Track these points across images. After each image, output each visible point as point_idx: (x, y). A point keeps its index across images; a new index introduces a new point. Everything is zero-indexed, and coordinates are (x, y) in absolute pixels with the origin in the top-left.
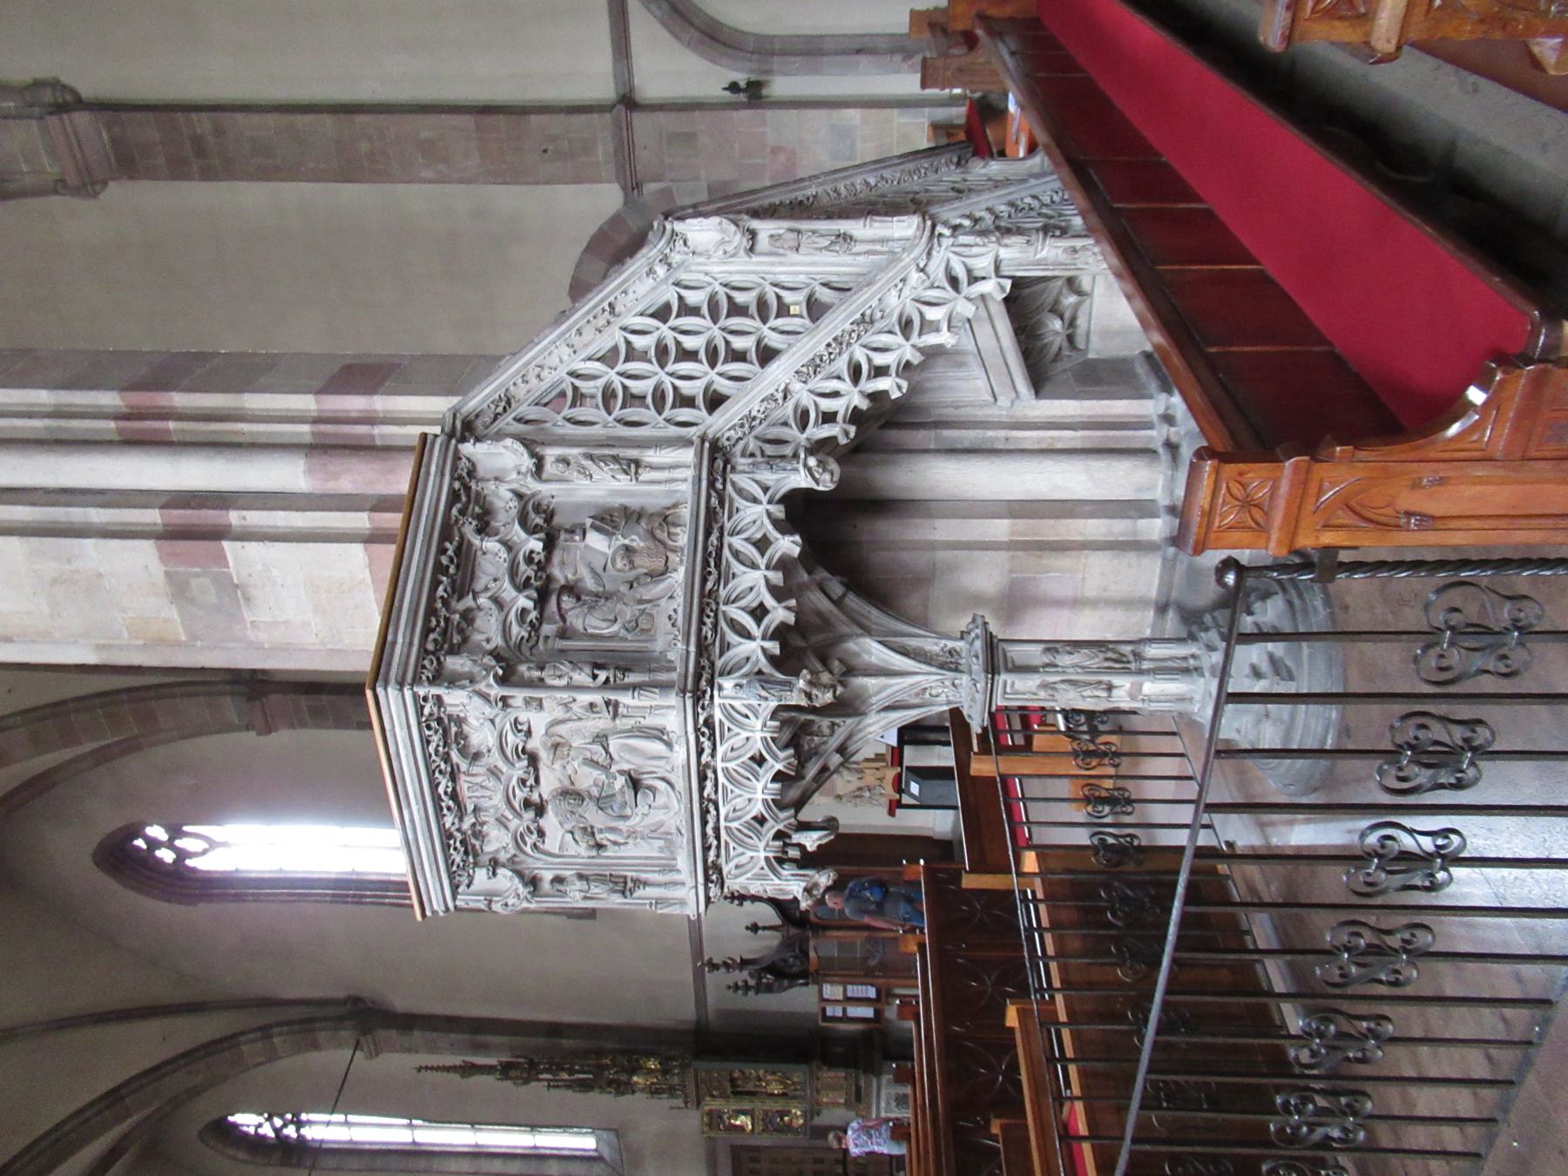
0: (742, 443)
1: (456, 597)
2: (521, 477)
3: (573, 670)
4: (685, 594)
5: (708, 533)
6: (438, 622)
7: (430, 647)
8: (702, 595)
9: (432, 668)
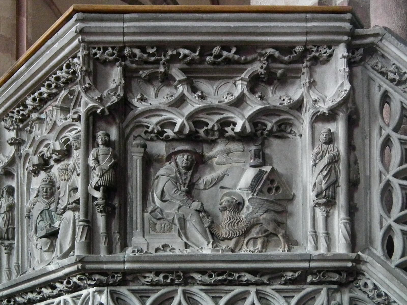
0: (365, 297)
1: (185, 66)
5: (253, 272)
6: (153, 55)
8: (186, 272)
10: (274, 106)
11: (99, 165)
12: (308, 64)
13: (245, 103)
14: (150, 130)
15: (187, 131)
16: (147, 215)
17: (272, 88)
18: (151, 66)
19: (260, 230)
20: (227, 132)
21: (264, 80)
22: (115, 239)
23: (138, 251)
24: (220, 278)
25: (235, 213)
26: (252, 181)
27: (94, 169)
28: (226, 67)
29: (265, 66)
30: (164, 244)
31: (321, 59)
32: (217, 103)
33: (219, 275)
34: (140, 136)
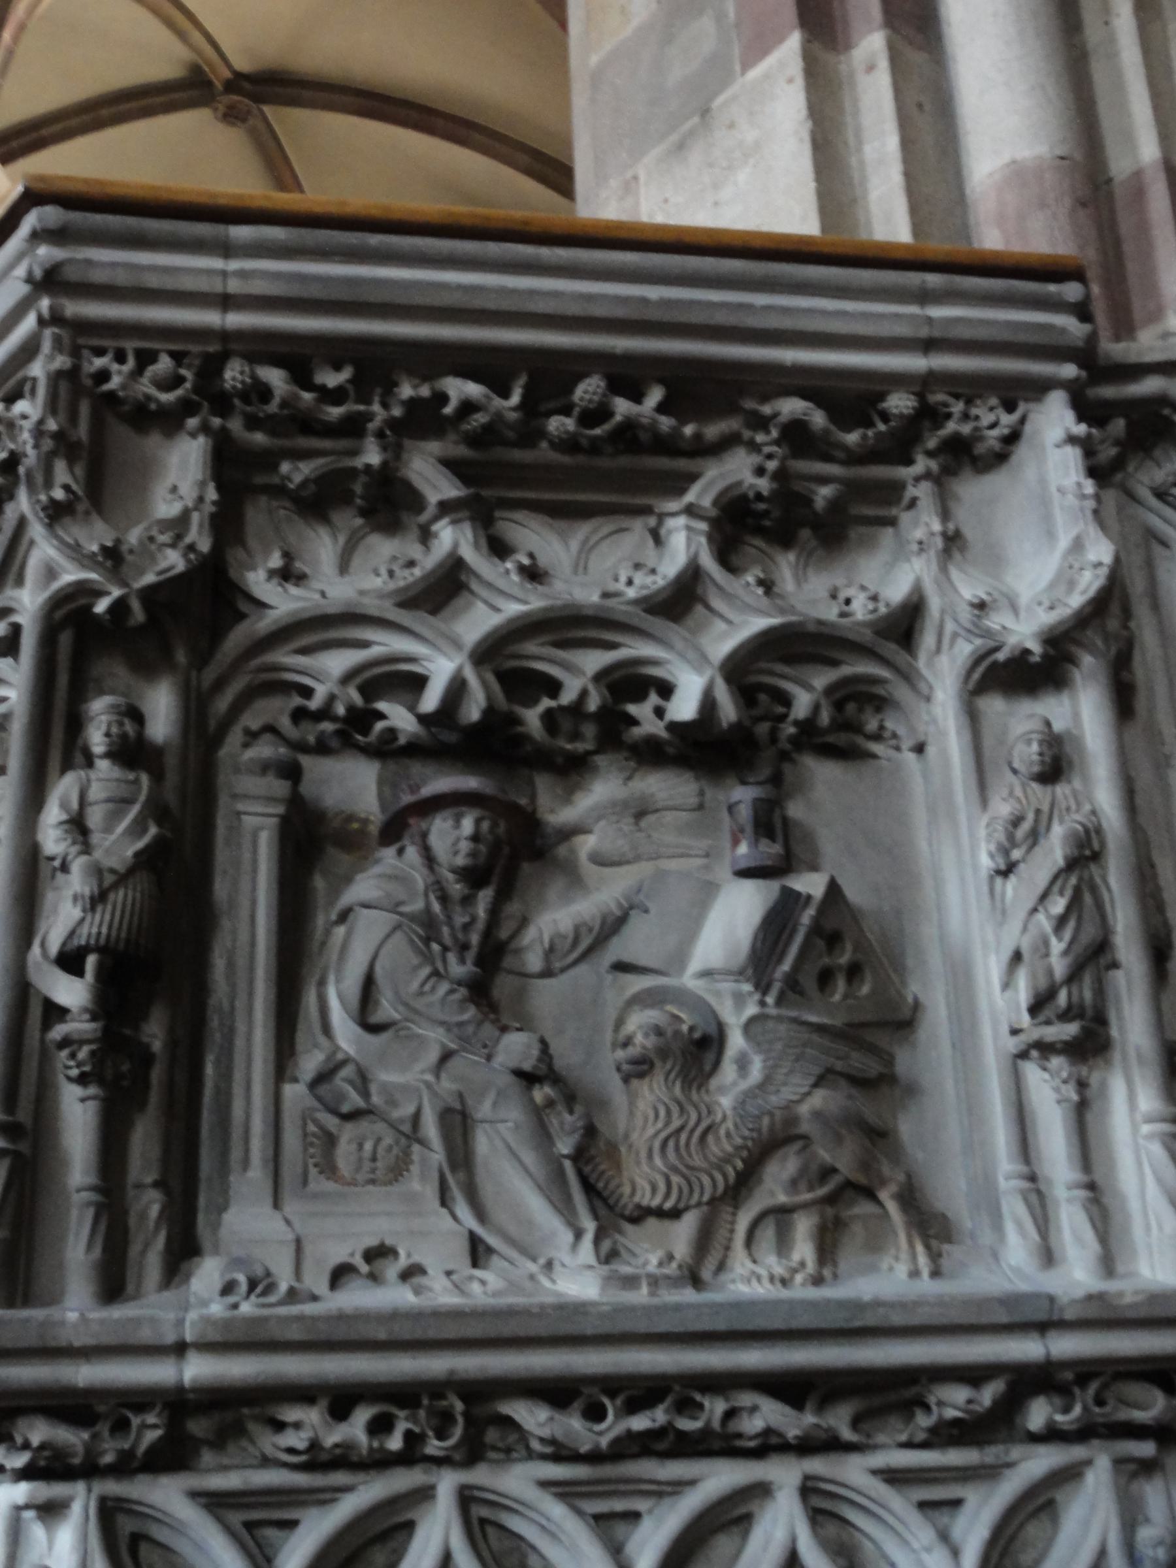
1: (462, 451)
2: (965, 614)
3: (97, 871)
4: (456, 1314)
7: (234, 374)
9: (145, 386)
10: (820, 622)
11: (87, 849)
12: (934, 465)
13: (699, 609)
14: (314, 704)
15: (473, 711)
16: (295, 1093)
17: (791, 556)
18: (327, 444)
19: (803, 1171)
20: (633, 722)
21: (767, 523)
22: (143, 1216)
23: (253, 1284)
24: (639, 1423)
25: (687, 1085)
26: (755, 938)
27: (65, 868)
28: (624, 461)
29: (772, 465)
30: (372, 1241)
31: (980, 449)
32: (595, 598)
33: (633, 1407)
34: (271, 729)
